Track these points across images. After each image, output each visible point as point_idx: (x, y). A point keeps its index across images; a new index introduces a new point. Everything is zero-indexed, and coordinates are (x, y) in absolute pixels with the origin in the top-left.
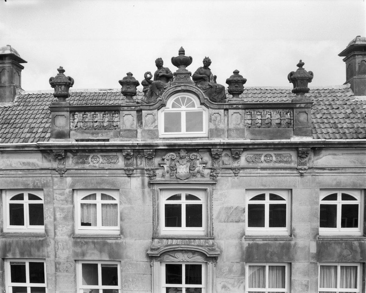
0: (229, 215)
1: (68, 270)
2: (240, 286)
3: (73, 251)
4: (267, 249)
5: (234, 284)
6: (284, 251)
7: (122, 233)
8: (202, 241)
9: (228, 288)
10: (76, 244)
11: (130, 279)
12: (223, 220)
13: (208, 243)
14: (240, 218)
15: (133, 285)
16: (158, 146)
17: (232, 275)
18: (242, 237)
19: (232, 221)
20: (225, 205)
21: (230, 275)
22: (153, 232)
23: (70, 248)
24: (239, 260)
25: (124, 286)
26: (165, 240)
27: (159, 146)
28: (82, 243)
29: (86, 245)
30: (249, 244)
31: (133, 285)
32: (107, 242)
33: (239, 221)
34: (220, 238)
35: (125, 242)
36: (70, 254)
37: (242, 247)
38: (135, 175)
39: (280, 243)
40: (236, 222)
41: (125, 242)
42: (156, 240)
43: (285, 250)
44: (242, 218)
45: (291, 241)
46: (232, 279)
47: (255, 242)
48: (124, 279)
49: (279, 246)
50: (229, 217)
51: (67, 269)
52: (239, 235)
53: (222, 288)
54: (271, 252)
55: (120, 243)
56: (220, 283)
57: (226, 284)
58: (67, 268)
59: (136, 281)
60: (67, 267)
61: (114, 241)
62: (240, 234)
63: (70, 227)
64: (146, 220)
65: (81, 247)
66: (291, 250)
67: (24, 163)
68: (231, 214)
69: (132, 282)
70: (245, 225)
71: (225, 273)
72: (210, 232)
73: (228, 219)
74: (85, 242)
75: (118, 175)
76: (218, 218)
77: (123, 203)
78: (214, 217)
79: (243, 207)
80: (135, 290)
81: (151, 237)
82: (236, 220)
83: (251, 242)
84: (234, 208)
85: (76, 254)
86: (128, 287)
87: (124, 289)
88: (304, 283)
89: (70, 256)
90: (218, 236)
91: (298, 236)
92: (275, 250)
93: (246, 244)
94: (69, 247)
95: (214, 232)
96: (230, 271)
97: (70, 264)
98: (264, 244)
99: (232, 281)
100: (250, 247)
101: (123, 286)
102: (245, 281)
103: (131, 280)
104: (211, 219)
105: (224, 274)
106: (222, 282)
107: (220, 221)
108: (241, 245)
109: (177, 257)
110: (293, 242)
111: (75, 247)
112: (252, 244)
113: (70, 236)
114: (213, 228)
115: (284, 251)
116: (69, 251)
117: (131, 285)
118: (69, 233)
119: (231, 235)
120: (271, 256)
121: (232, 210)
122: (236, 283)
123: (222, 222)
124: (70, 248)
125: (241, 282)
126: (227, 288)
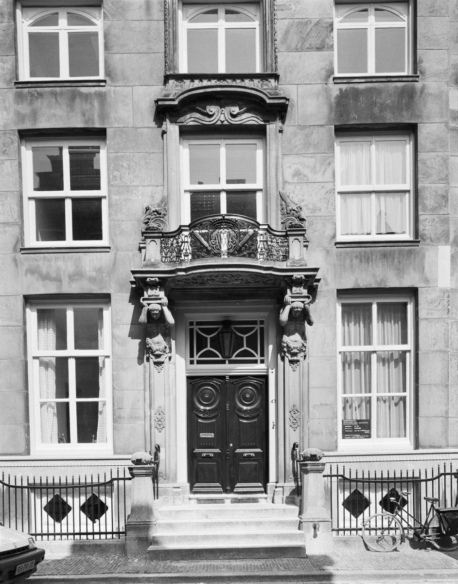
0: (305, 36)
1: (5, 151)
3: (15, 111)
4: (374, 99)
5: (315, 167)
6: (404, 101)
7: (108, 73)
8: (256, 81)
9: (305, 176)
10: (19, 98)
11: (123, 164)
12: (293, 45)
13: (267, 85)
14: (324, 41)
15: (129, 174)
18: (329, 77)
19: (310, 49)
21: (307, 150)
22: (165, 66)
23: (9, 107)
25: (113, 178)
26: (187, 82)
28: (32, 95)
29: (39, 100)
30: (341, 90)
31: (129, 174)
32: (80, 91)
33: (324, 47)
34: (288, 79)
35: (114, 92)
36: (10, 119)
37: (328, 96)
39: (396, 87)
40: (319, 49)
41: (114, 92)
42: (171, 82)
43: (406, 99)
44: (327, 40)
45: (416, 83)
46: (311, 157)
47: (351, 85)
48: (113, 165)
49: (395, 92)
50: (304, 40)
51: (4, 149)
52: (324, 73)
53: (294, 175)
54: (382, 104)
55: (105, 93)
56: (290, 167)
57: (301, 168)
58: (4, 146)
59: (135, 168)
60: (4, 144)
61: (93, 90)
62: (325, 71)
63: (9, 65)
64: (152, 47)
65: (31, 102)
66: (417, 98)
68: (308, 35)
69: (128, 169)
70: (333, 55)
71: (298, 148)
72: (272, 65)
73: (302, 44)
74: (38, 93)
77: (109, 15)
78: (279, 36)
79: (330, 21)
80: (133, 185)
81: (162, 75)
82: (317, 46)
83: (344, 87)
84: (314, 22)
85: (21, 117)
86: (121, 179)
87: (112, 183)
89: (9, 122)
91: (427, 72)
93: (335, 90)
94: (7, 105)
95: (279, 64)
97: (10, 138)
98: (369, 90)
99: (310, 161)
100: (343, 95)
101: (111, 177)
102: (334, 162)
103: (125, 165)
104: (274, 40)
105: (297, 149)
106: (293, 164)
107: (289, 50)
108: (327, 91)
109: (211, 113)
110: (418, 85)
111: (18, 104)
112: (346, 90)
113: (8, 82)
114: (276, 57)
115: (404, 101)
116: (8, 113)
117: (127, 175)
118: (8, 77)
119: (308, 74)
120: (381, 111)
121: (310, 26)
122: (318, 166)
124: (9, 107)
125: (328, 161)
126: (302, 175)
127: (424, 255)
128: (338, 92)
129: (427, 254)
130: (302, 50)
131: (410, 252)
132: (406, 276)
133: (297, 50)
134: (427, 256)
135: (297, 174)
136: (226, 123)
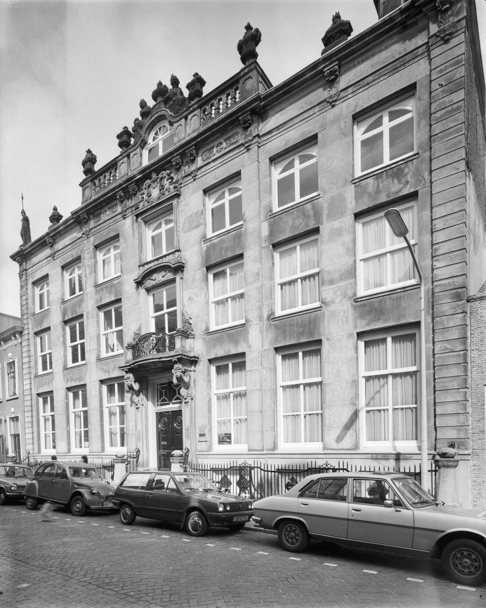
2: (201, 294)
16: (135, 176)
17: (196, 284)
20: (189, 214)
24: (200, 266)
27: (136, 177)
37: (202, 253)
38: (128, 215)
40: (197, 227)
47: (211, 242)
52: (199, 239)
53: (189, 300)
67: (71, 239)
75: (118, 220)
76: (183, 229)
83: (208, 244)
88: (255, 271)
90: (184, 247)
92: (229, 245)
93: (204, 246)
96: (194, 280)
98: (220, 242)
100: (208, 248)
108: (201, 249)
110: (243, 229)
112: (210, 246)
120: (225, 252)
123: (186, 233)
127: (248, 333)
128: (206, 248)
129: (250, 330)
130: (190, 230)
131: (241, 331)
132: (239, 346)
133: (188, 231)
134: (250, 332)
135: (190, 299)
136: (161, 281)
